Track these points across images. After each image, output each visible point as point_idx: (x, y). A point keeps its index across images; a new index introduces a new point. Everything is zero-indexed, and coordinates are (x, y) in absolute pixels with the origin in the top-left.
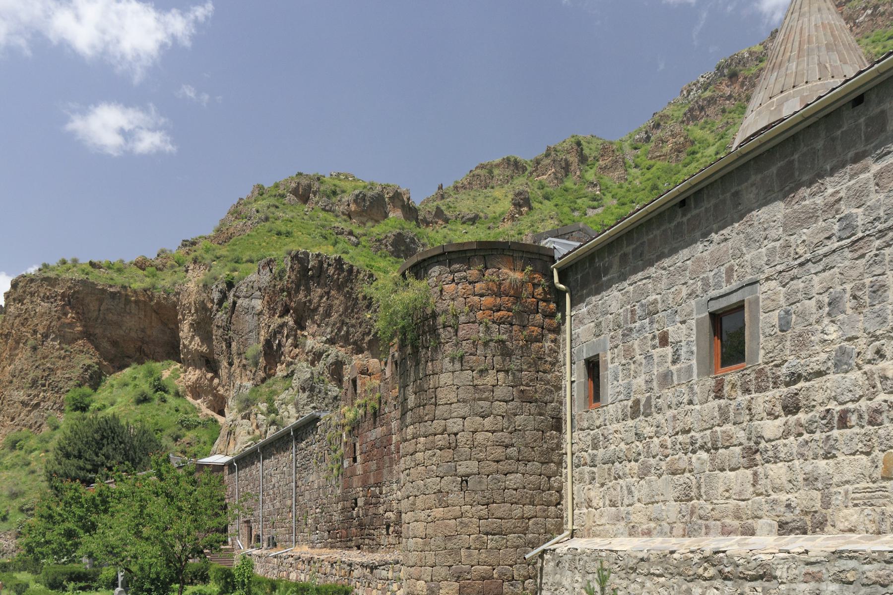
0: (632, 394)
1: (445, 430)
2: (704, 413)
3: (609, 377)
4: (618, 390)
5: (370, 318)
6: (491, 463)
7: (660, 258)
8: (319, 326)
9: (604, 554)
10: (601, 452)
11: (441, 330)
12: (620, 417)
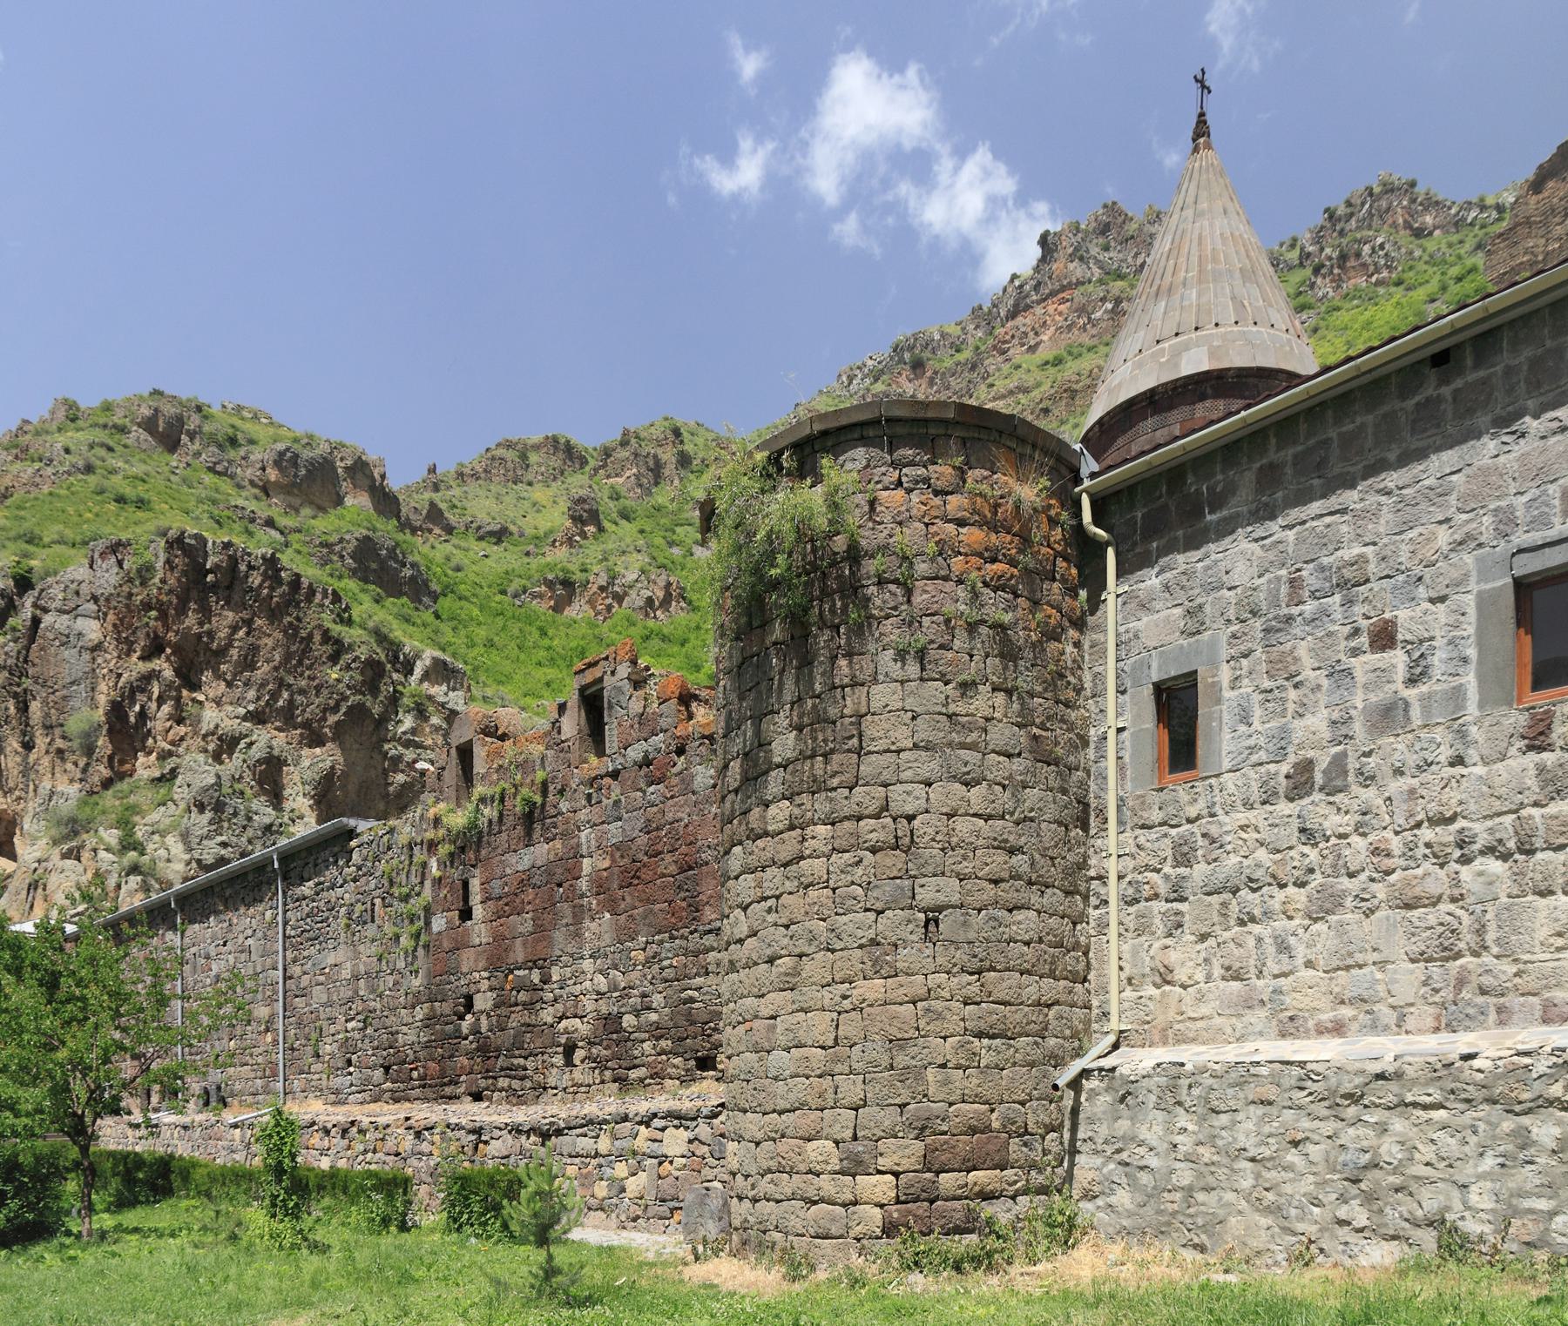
0: (1290, 749)
2: (1497, 781)
3: (1226, 717)
4: (1251, 742)
5: (338, 680)
6: (985, 884)
8: (229, 684)
12: (1256, 795)
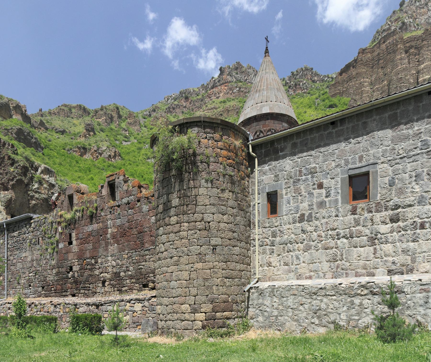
0: (299, 211)
1: (203, 219)
2: (345, 221)
3: (284, 202)
4: (290, 208)
6: (227, 240)
7: (318, 147)
9: (294, 287)
10: (278, 239)
11: (199, 164)
12: (291, 221)
